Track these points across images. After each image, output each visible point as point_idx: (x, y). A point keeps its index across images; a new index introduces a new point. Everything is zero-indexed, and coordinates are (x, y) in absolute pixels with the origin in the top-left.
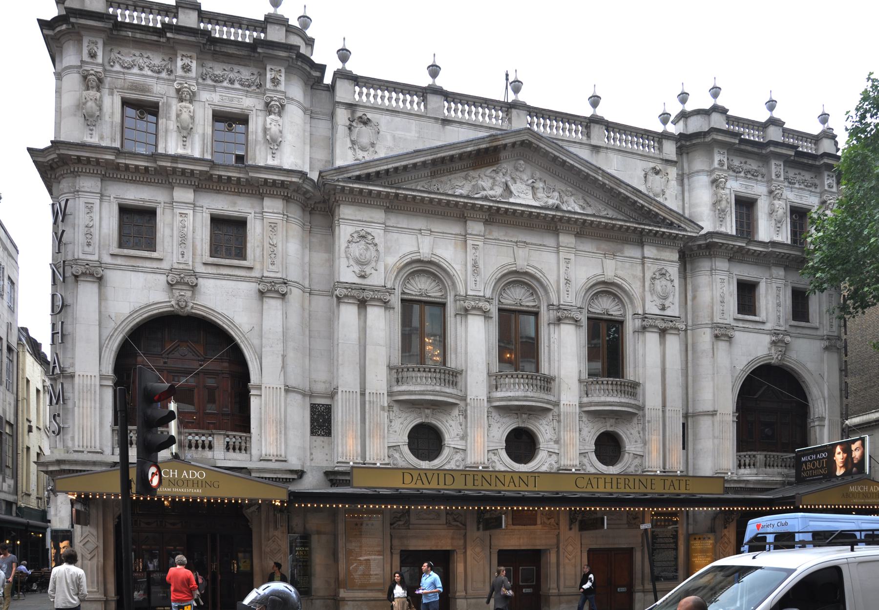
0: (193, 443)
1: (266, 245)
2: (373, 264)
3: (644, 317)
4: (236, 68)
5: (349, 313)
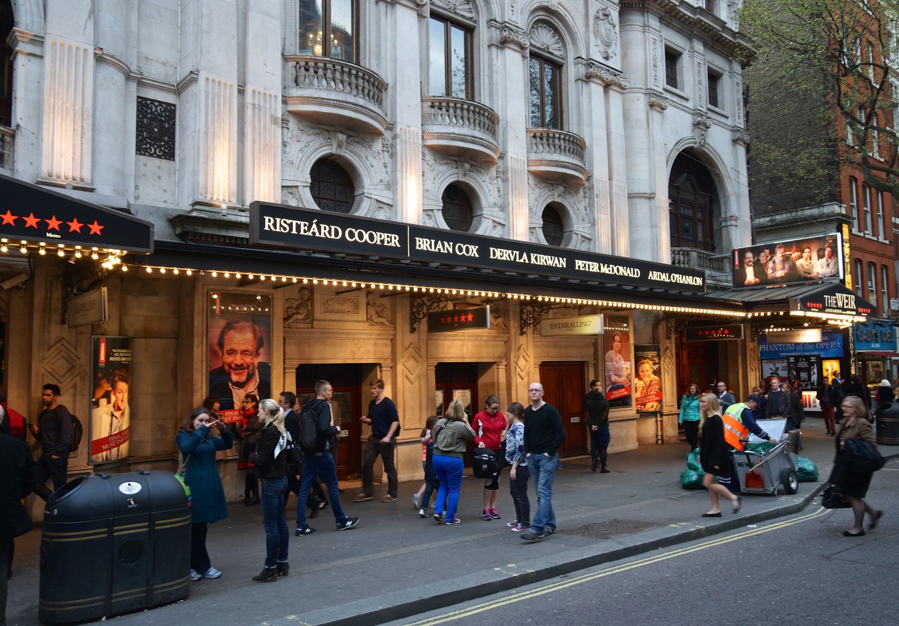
3: (590, 63)
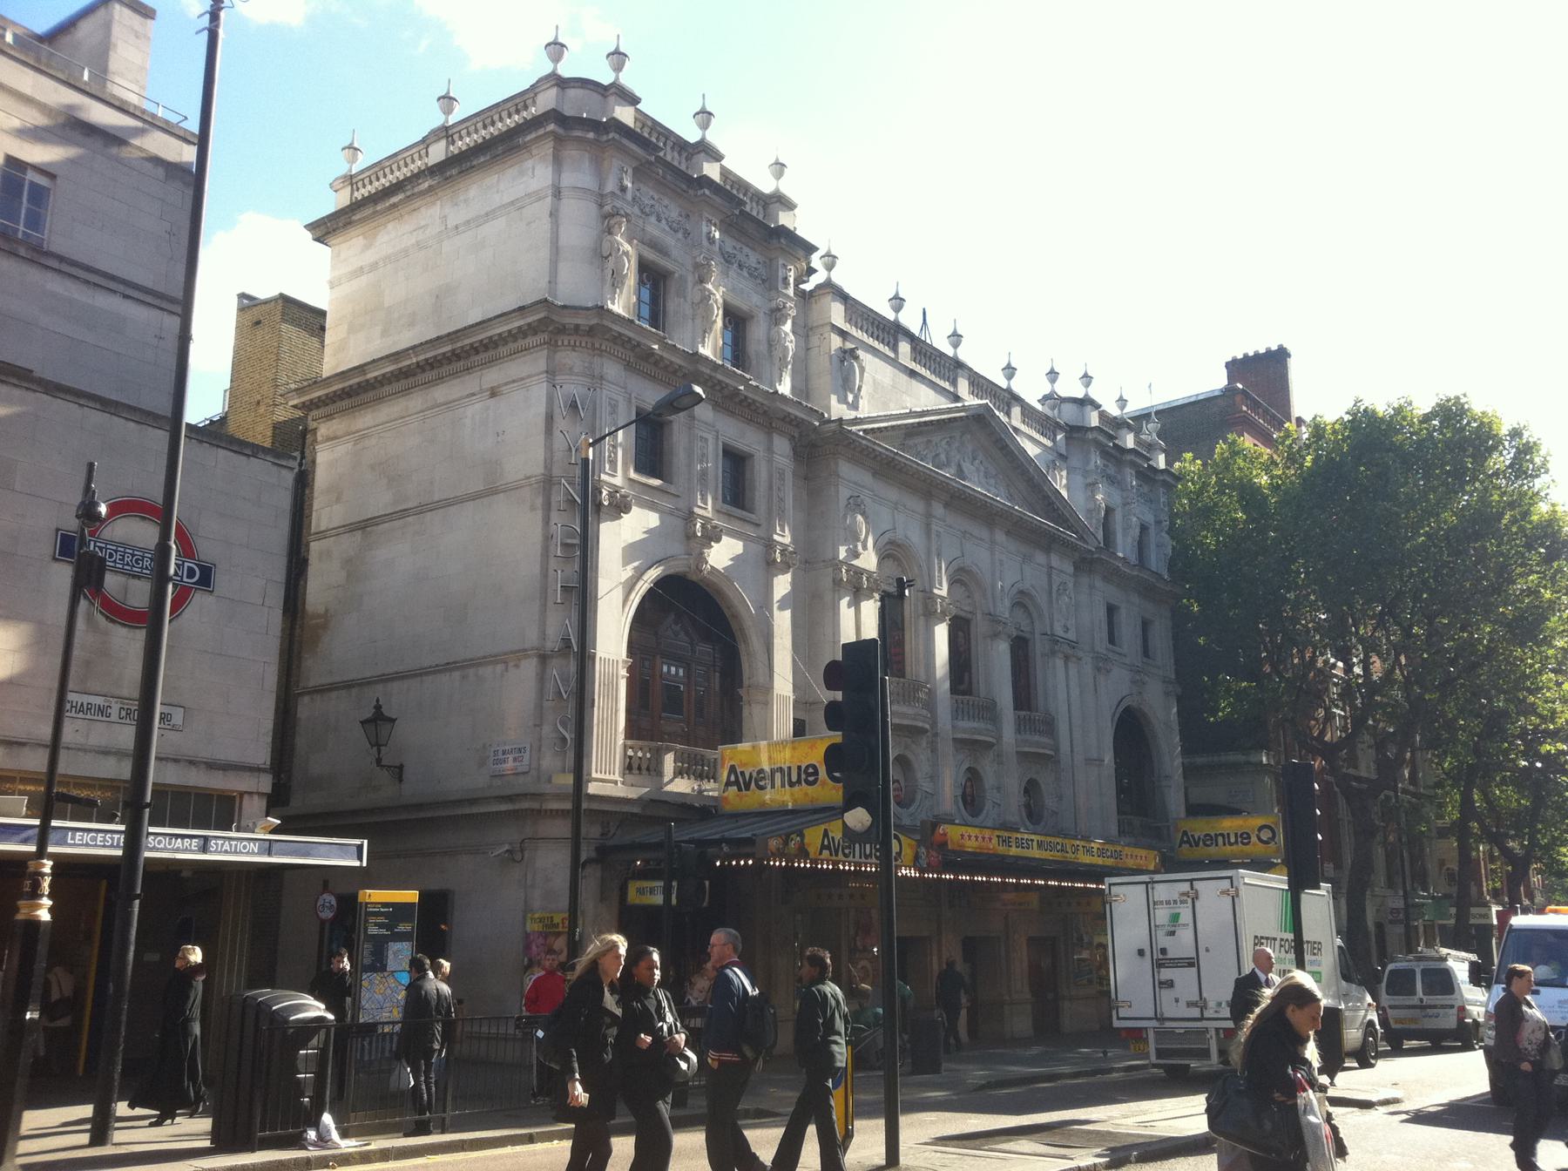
4: (746, 250)
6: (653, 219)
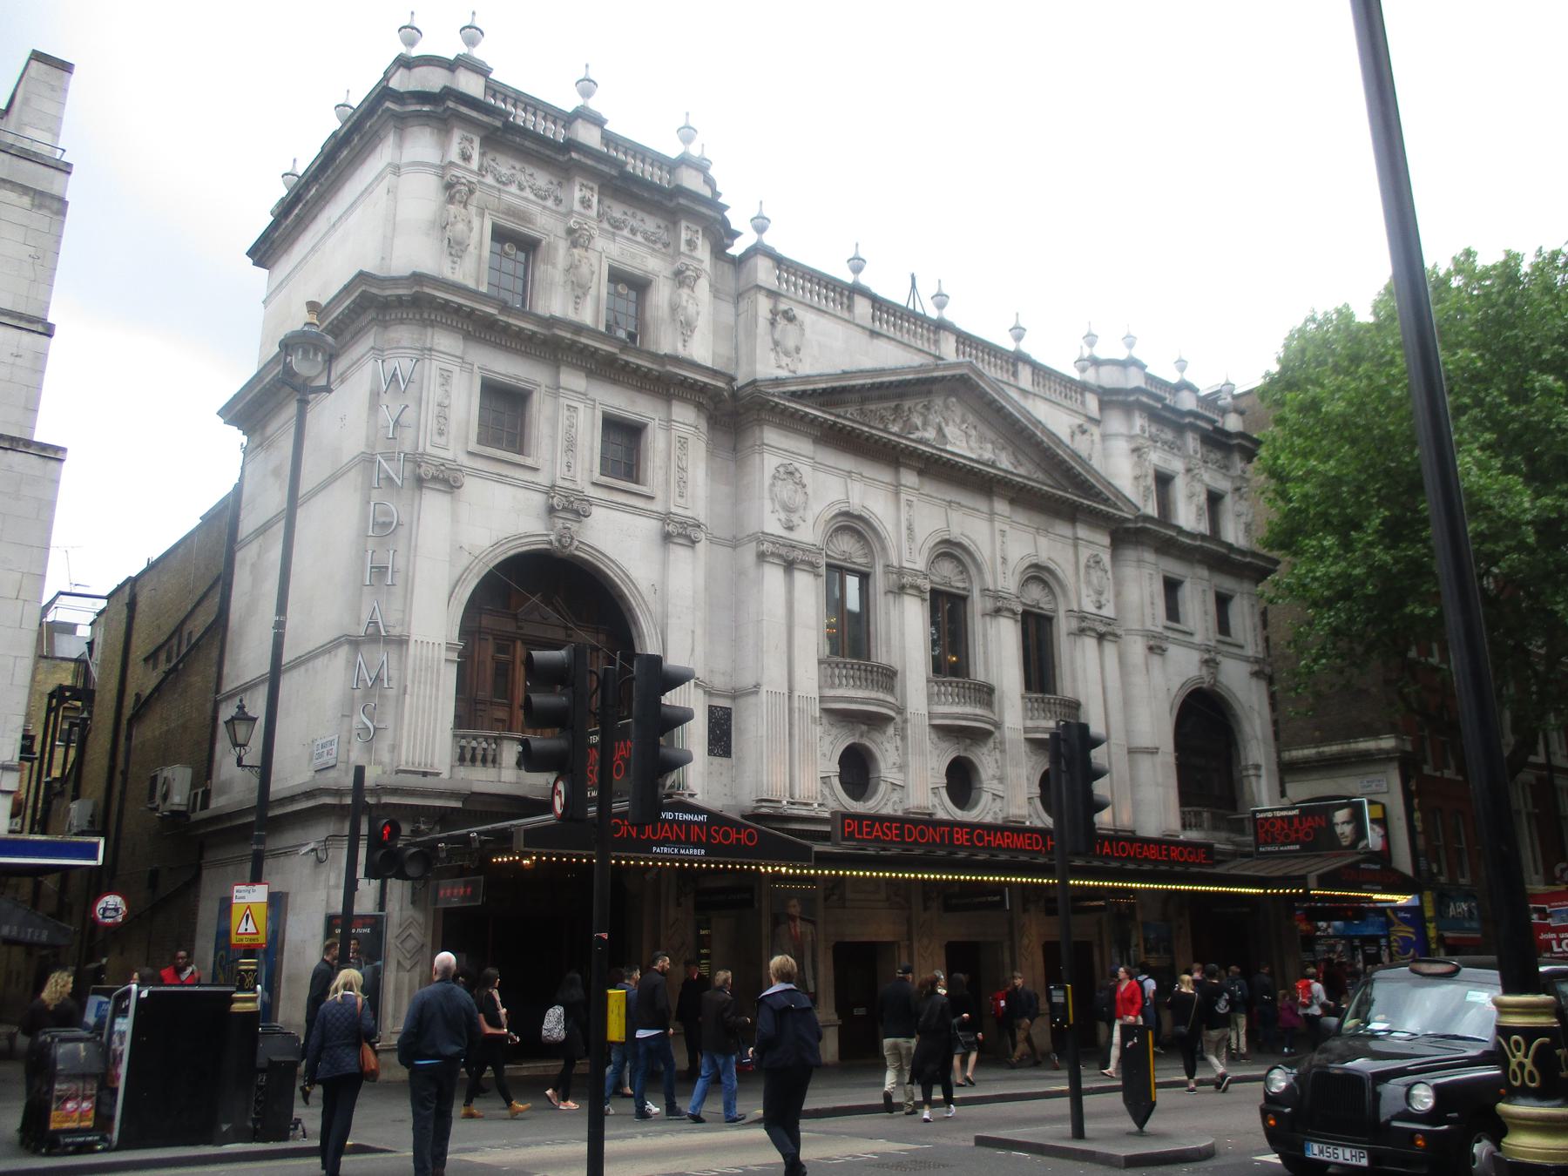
0: (479, 753)
1: (674, 468)
2: (801, 512)
4: (640, 214)
5: (773, 576)
6: (513, 189)
